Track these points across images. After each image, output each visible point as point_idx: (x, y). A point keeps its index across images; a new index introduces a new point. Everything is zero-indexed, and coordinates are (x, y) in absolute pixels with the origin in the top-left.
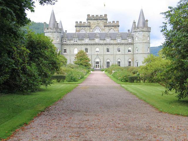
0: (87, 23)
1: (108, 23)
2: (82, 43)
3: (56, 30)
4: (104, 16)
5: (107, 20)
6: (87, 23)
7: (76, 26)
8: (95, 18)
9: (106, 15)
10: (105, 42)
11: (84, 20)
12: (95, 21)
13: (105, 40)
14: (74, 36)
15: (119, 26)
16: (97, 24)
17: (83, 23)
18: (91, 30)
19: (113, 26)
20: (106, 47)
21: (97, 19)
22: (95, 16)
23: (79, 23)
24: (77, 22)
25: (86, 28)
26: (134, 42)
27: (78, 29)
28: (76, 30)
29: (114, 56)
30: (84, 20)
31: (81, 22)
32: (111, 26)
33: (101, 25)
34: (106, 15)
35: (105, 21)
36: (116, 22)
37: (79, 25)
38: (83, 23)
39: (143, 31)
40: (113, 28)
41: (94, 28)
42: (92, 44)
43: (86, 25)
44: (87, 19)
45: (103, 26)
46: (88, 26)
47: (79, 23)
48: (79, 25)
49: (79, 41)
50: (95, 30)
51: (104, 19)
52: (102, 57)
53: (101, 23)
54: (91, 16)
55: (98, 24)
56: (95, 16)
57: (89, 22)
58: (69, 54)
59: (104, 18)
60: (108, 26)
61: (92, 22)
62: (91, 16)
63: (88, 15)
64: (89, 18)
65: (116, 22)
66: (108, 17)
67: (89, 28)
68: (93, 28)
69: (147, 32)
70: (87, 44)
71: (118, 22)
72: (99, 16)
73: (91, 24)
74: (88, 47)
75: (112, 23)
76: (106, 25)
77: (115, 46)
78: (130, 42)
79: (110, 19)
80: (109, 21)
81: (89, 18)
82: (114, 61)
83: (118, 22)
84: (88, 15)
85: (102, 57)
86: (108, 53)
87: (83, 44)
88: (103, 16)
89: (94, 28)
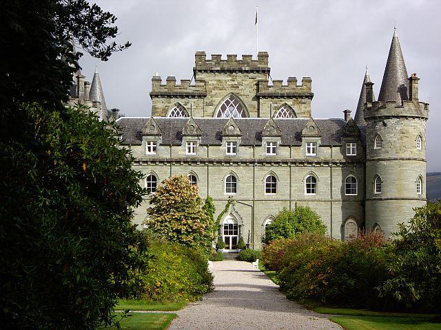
0: (193, 83)
1: (270, 83)
2: (175, 156)
4: (256, 59)
5: (266, 71)
6: (193, 83)
7: (153, 95)
8: (226, 67)
9: (263, 56)
10: (261, 153)
11: (183, 71)
12: (223, 77)
14: (147, 131)
15: (311, 96)
16: (232, 86)
17: (178, 83)
18: (210, 109)
19: (289, 97)
20: (263, 173)
21: (231, 71)
22: (224, 58)
23: (164, 82)
24: (156, 80)
25: (192, 101)
26: (368, 157)
27: (161, 103)
28: (154, 108)
30: (183, 71)
31: (171, 80)
32: (283, 96)
34: (263, 56)
35: (260, 77)
36: (299, 83)
37: (164, 90)
38: (178, 83)
39: (398, 117)
40: (290, 102)
41: (220, 103)
42: (211, 162)
43: (190, 90)
44: (194, 71)
45: (253, 94)
46: (200, 96)
47: (164, 82)
48: (164, 91)
49: (163, 147)
50: (223, 108)
51: (258, 72)
53: (246, 86)
54: (209, 57)
56: (224, 58)
57: (201, 81)
59: (257, 67)
60: (271, 96)
61: (211, 79)
62: (209, 57)
63: (200, 56)
64: (203, 65)
65: (299, 83)
66: (271, 64)
67: (201, 101)
68: (217, 100)
70: (194, 162)
71: (307, 81)
72: (239, 58)
73: (209, 87)
74: (199, 170)
75: (285, 83)
76: (263, 91)
77: (294, 169)
78: (351, 154)
79: (280, 71)
80: (274, 76)
81: (203, 65)
83: (307, 81)
84: (200, 56)
86: (311, 194)
87: (178, 162)
88: (255, 58)
89: (220, 103)
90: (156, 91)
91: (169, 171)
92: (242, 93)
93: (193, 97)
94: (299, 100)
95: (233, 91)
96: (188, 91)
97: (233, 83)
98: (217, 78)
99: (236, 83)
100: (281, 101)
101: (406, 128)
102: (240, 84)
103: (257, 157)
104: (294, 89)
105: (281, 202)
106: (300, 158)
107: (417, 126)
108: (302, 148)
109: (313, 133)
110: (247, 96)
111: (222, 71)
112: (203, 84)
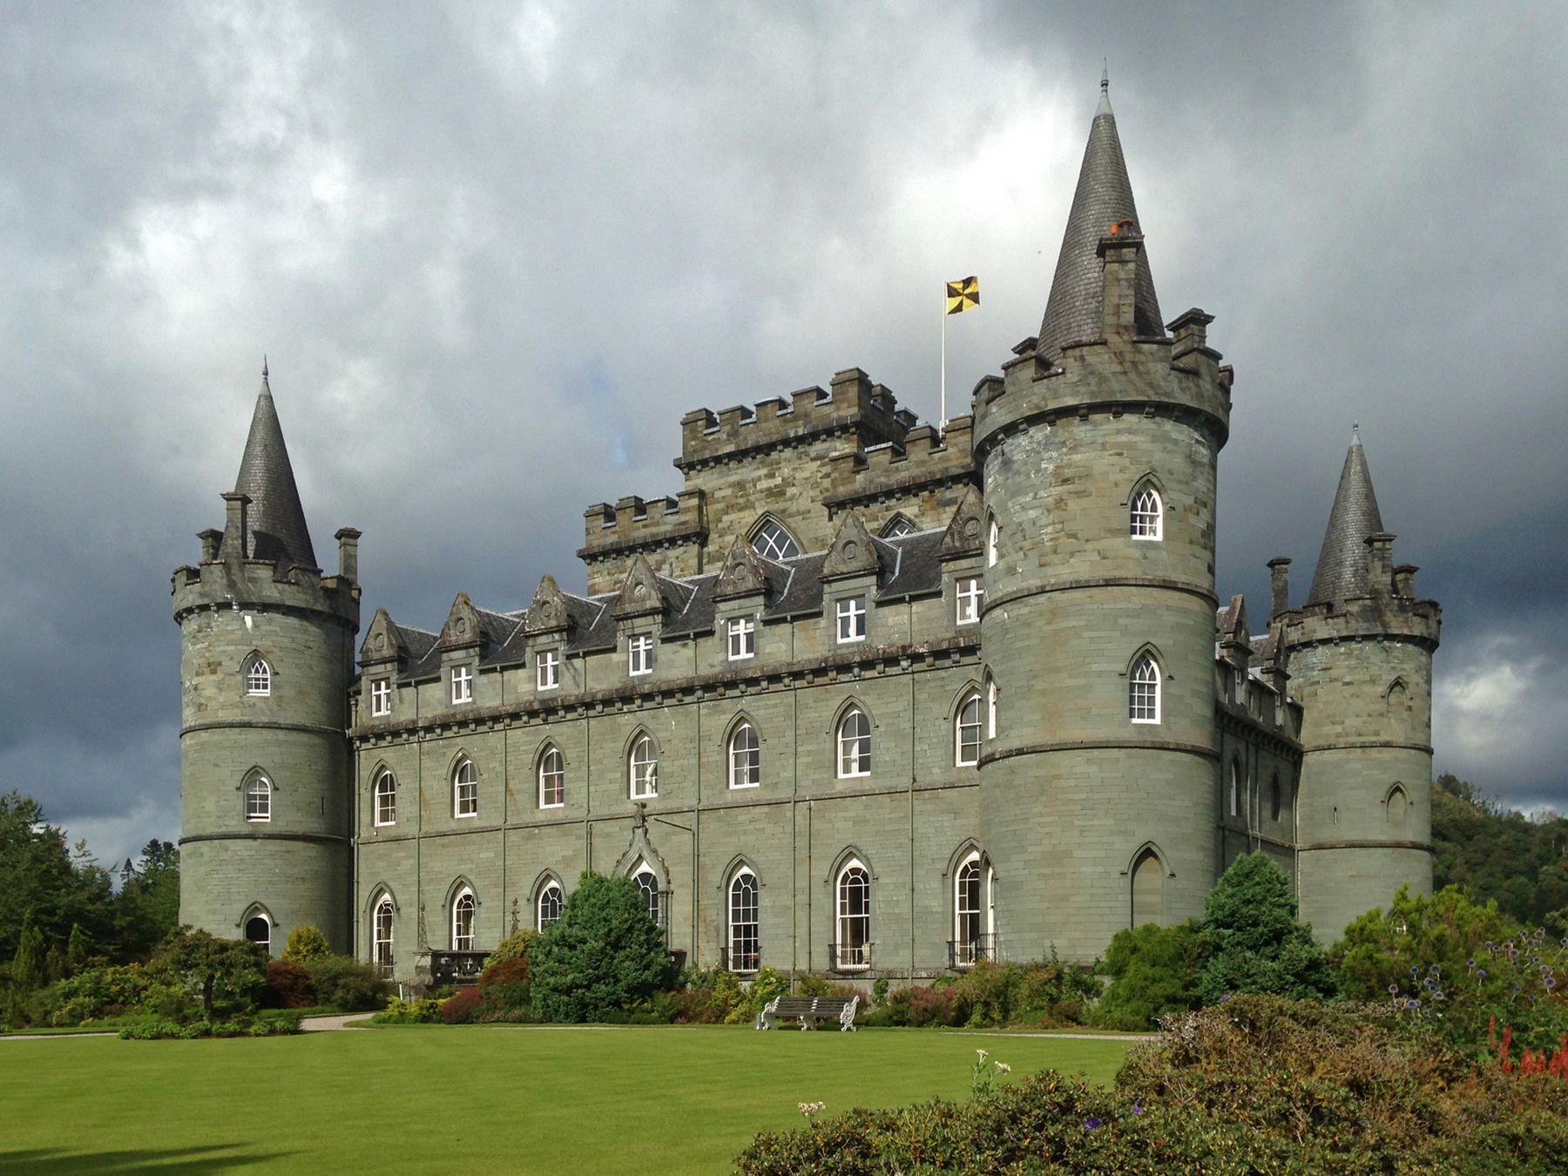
3: (232, 586)
12: (749, 471)
13: (711, 633)
20: (716, 717)
25: (672, 553)
29: (801, 822)
32: (889, 494)
33: (803, 503)
52: (688, 837)
55: (777, 493)
58: (413, 830)
69: (1130, 419)
70: (547, 710)
74: (563, 732)
76: (843, 491)
82: (802, 883)
85: (688, 837)
90: (596, 543)
91: (501, 746)
92: (793, 507)
93: (672, 542)
94: (938, 493)
95: (774, 507)
96: (663, 529)
97: (771, 483)
98: (734, 478)
99: (778, 480)
100: (887, 509)
101: (1076, 457)
102: (787, 483)
103: (705, 671)
104: (923, 462)
105: (766, 809)
106: (817, 655)
107: (1131, 446)
108: (823, 622)
109: (854, 566)
110: (805, 514)
111: (739, 456)
112: (695, 501)
